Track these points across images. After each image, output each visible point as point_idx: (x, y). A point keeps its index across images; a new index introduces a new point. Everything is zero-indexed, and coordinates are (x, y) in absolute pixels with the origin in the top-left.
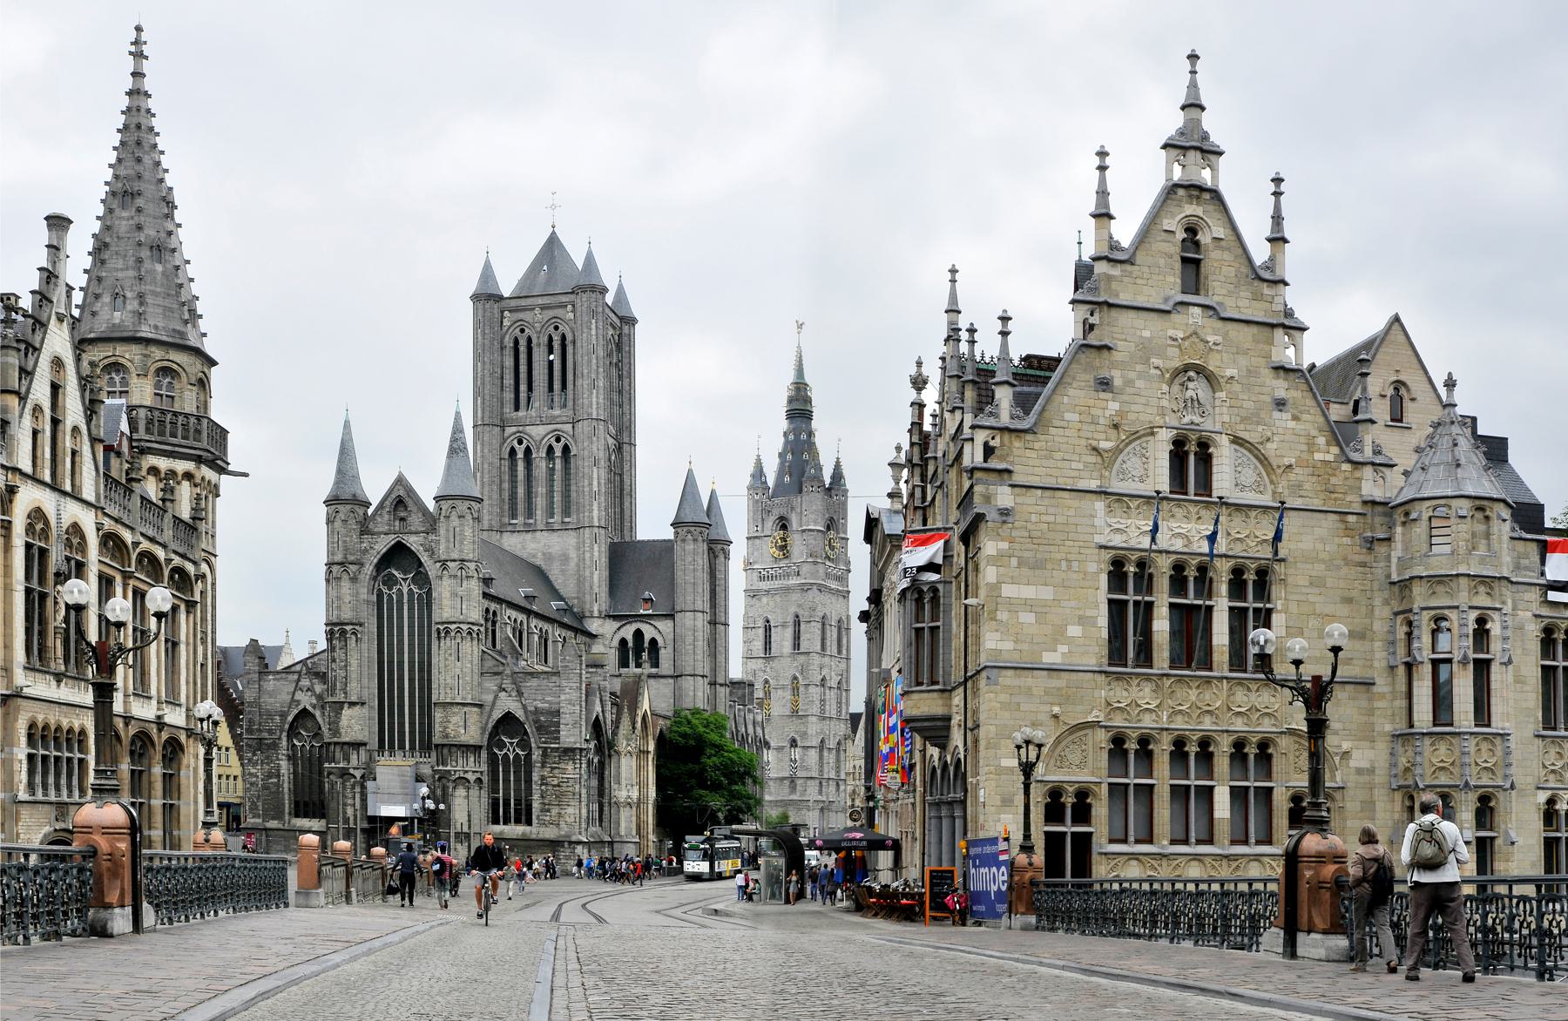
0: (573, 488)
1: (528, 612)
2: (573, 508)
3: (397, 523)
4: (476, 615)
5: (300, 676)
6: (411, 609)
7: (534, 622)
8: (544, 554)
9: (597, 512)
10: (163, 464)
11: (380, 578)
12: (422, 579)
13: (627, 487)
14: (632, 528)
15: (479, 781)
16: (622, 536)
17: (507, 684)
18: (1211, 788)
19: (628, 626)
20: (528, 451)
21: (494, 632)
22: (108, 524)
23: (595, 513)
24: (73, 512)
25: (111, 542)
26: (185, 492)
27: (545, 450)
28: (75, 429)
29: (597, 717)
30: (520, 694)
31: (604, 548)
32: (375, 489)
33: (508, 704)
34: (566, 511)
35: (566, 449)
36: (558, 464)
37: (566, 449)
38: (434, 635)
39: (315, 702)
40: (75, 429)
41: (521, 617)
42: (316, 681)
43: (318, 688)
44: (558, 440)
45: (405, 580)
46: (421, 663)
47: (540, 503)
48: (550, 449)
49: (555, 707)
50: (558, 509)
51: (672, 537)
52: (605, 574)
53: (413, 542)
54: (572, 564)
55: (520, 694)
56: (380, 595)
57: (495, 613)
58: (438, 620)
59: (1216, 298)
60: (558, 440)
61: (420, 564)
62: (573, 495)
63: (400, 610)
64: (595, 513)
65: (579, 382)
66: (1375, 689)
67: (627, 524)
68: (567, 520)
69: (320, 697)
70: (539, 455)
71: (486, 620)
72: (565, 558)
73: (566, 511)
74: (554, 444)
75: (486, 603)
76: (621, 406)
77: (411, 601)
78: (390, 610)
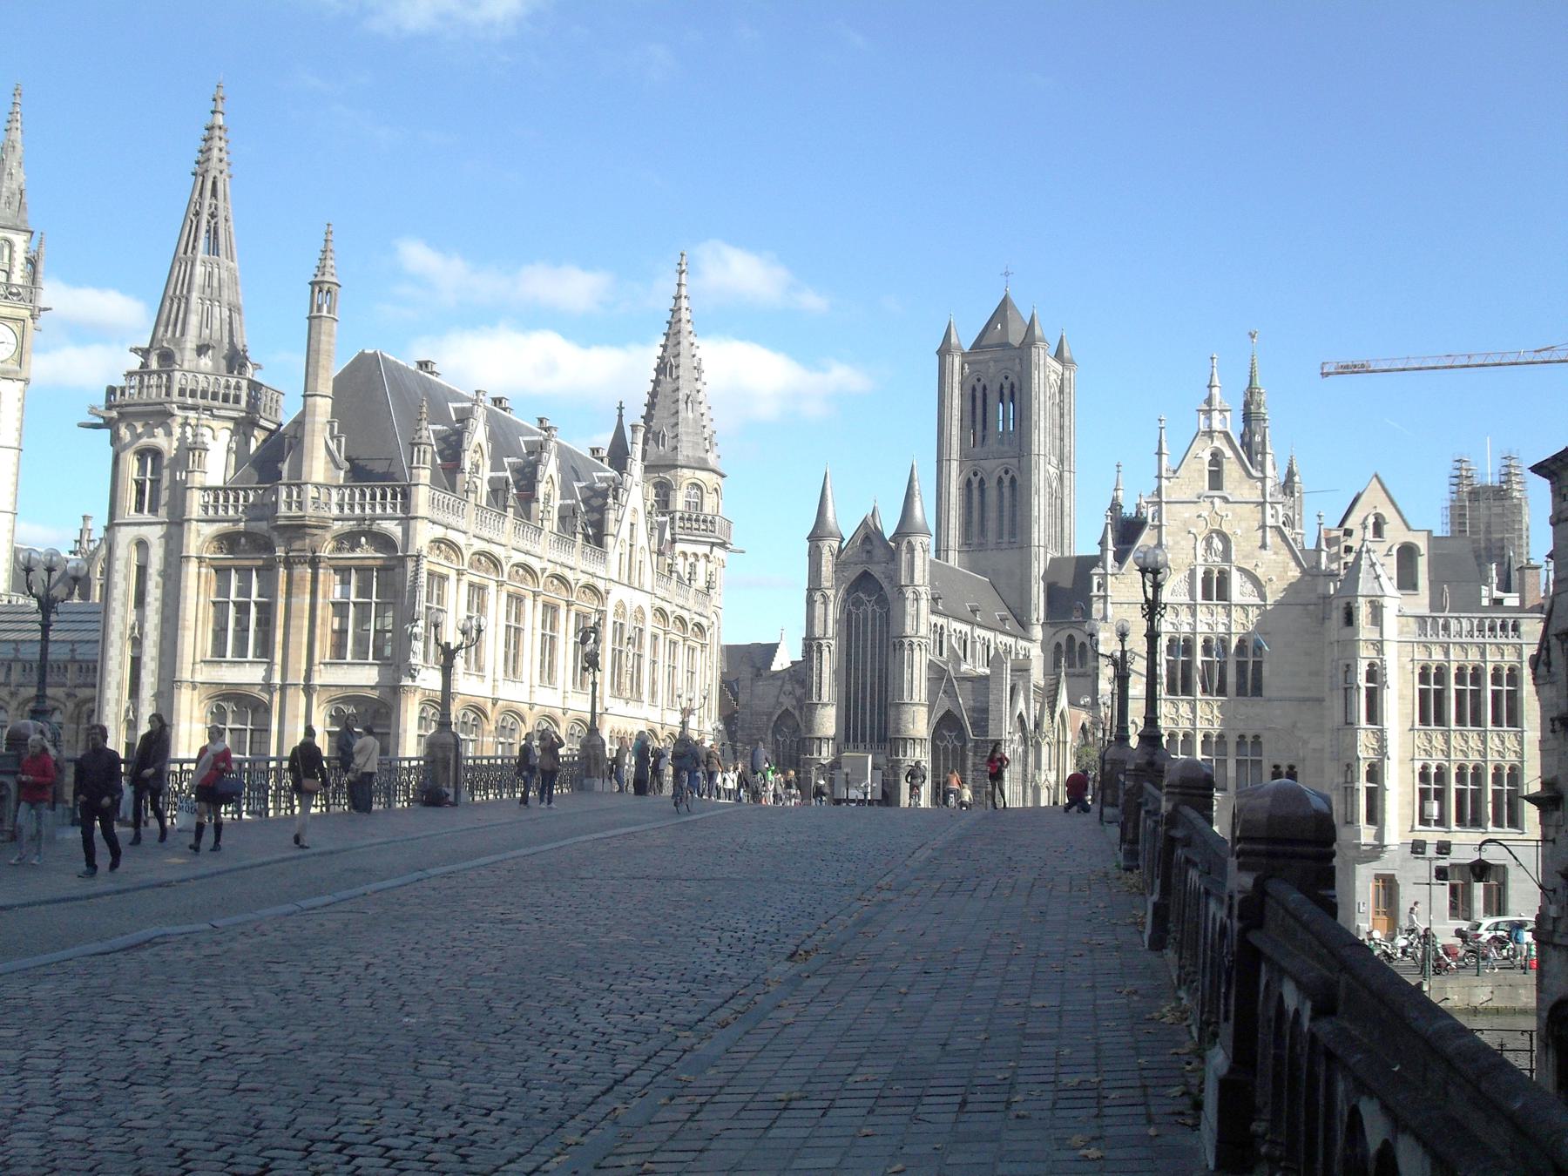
0: (1018, 513)
1: (971, 623)
3: (864, 555)
5: (783, 682)
6: (874, 625)
7: (979, 632)
8: (993, 570)
10: (690, 548)
11: (850, 600)
12: (882, 601)
13: (1066, 510)
16: (1062, 553)
18: (1226, 760)
19: (1062, 632)
20: (982, 481)
21: (941, 642)
22: (659, 603)
24: (646, 602)
25: (661, 612)
26: (701, 566)
27: (996, 481)
28: (642, 548)
29: (1021, 713)
32: (846, 522)
34: (1013, 534)
35: (1013, 480)
36: (1007, 491)
37: (1013, 480)
38: (891, 648)
39: (795, 703)
40: (642, 548)
41: (966, 628)
42: (796, 686)
43: (799, 692)
44: (1006, 472)
45: (869, 601)
46: (880, 670)
47: (992, 525)
48: (1000, 480)
50: (1006, 532)
51: (1098, 553)
53: (877, 571)
56: (849, 615)
57: (942, 627)
58: (895, 635)
59: (1229, 491)
60: (1006, 472)
61: (882, 588)
63: (865, 625)
66: (1324, 703)
67: (1066, 541)
68: (1013, 540)
69: (799, 700)
70: (991, 485)
71: (935, 632)
73: (1013, 534)
74: (1004, 476)
75: (934, 619)
76: (1062, 440)
77: (874, 619)
78: (857, 627)
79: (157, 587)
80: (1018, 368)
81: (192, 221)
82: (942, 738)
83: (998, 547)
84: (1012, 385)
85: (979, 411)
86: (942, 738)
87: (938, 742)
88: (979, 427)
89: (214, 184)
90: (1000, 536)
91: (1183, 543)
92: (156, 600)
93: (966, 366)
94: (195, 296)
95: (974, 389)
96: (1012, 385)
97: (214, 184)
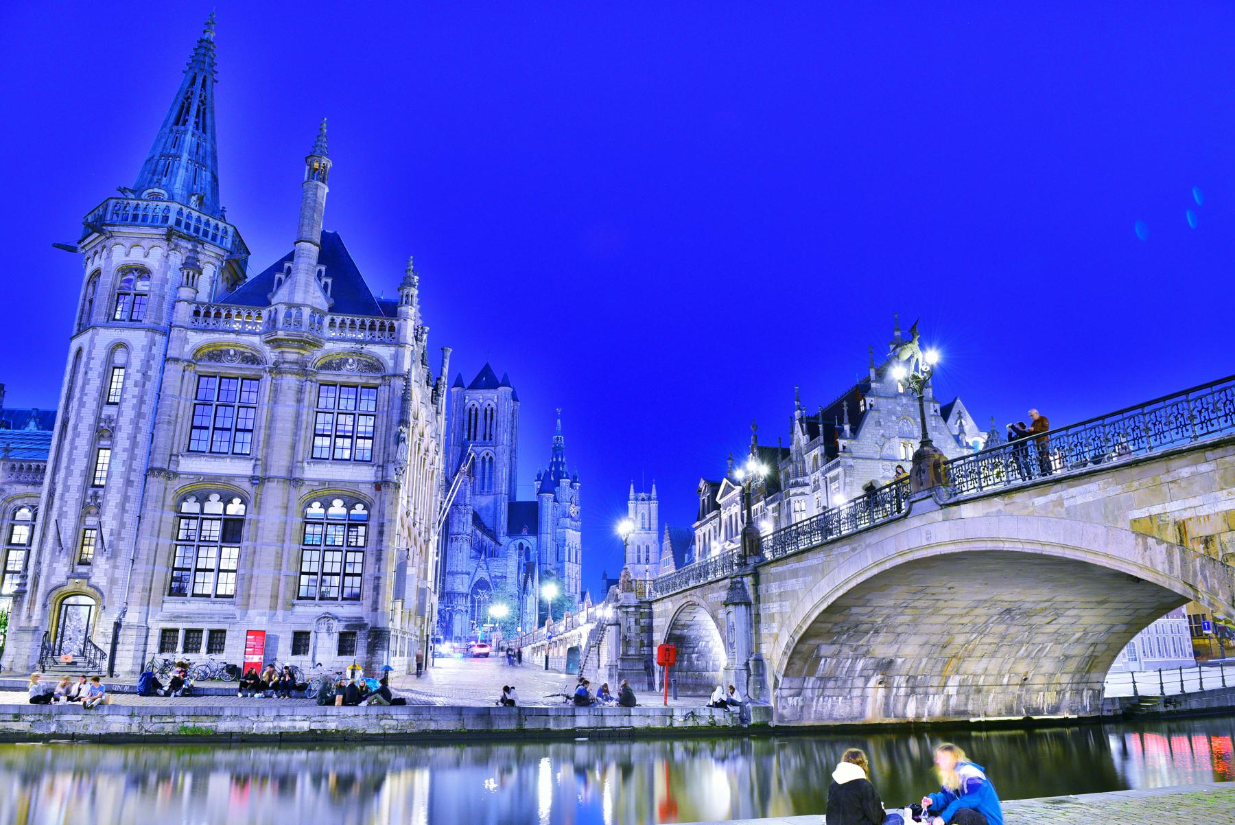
0: (493, 476)
2: (493, 485)
4: (469, 531)
9: (504, 488)
14: (515, 496)
15: (467, 611)
17: (482, 563)
23: (504, 488)
30: (488, 569)
31: (507, 504)
33: (482, 574)
34: (490, 487)
36: (487, 465)
44: (487, 454)
49: (504, 575)
50: (486, 486)
52: (506, 516)
54: (491, 511)
55: (488, 569)
62: (493, 479)
64: (504, 488)
65: (498, 429)
72: (487, 508)
73: (490, 487)
79: (136, 385)
80: (496, 400)
81: (184, 103)
82: (477, 594)
83: (481, 494)
84: (492, 409)
85: (473, 422)
86: (477, 594)
87: (474, 596)
88: (472, 430)
89: (204, 81)
90: (483, 488)
91: (890, 424)
92: (134, 397)
93: (467, 397)
94: (185, 156)
95: (470, 410)
96: (492, 409)
97: (204, 81)
